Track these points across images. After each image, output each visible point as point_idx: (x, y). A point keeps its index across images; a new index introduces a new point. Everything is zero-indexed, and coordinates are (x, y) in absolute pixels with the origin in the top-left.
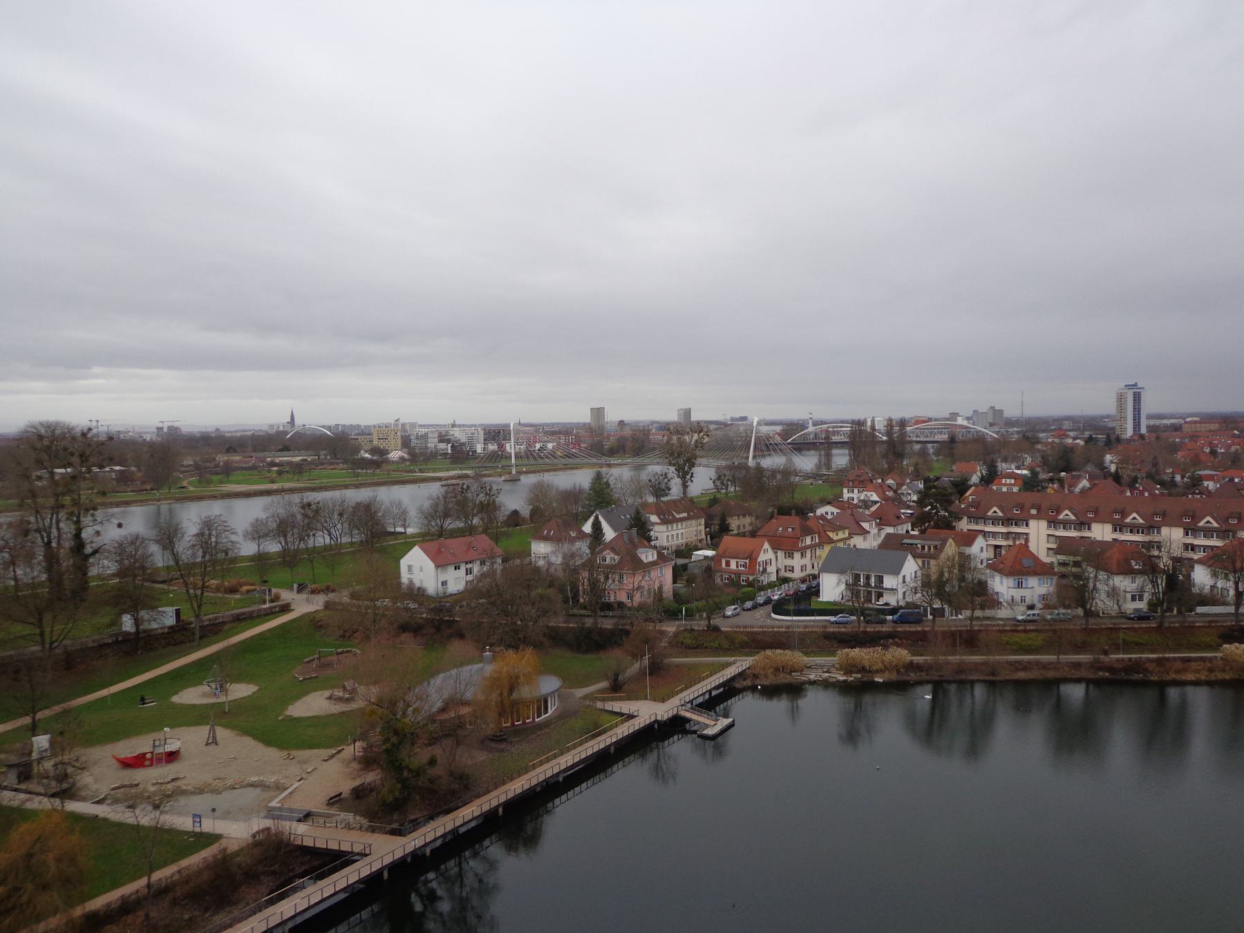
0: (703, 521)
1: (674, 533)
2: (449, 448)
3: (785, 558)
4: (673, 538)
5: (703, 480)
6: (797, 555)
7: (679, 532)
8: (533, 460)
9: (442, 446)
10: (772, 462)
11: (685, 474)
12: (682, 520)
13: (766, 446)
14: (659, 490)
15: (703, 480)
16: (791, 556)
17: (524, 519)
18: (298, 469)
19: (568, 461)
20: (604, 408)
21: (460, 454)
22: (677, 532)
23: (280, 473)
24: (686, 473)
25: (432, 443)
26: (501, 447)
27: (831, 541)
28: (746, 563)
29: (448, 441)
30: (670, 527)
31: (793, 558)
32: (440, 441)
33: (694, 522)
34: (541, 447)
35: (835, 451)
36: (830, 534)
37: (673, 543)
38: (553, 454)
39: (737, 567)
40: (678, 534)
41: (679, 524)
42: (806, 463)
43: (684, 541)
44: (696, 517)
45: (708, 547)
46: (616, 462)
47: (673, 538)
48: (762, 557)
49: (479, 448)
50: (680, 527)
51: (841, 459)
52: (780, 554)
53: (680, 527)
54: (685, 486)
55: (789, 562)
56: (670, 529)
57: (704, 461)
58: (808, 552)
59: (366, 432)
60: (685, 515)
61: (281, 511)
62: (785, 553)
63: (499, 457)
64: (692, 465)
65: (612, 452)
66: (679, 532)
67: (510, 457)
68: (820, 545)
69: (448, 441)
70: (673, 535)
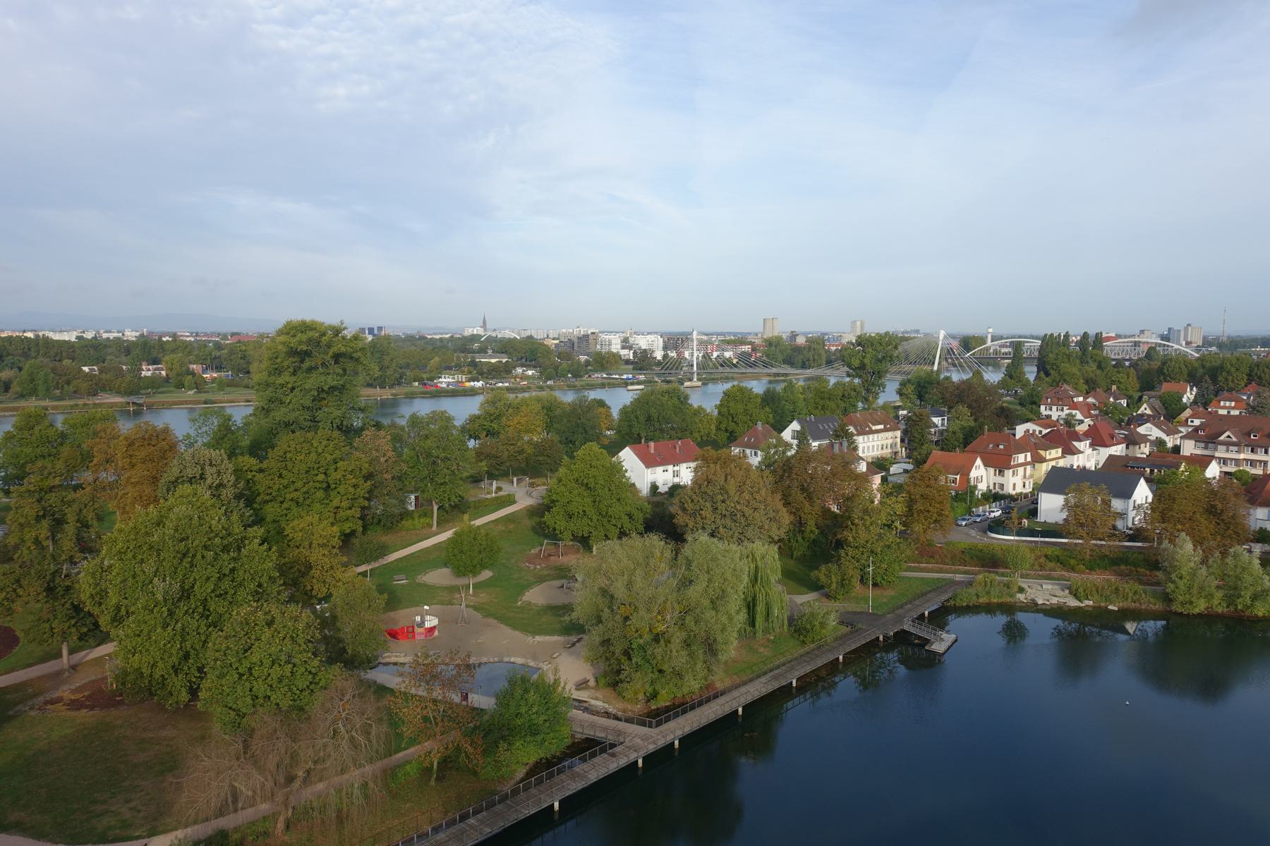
1: (870, 444)
2: (631, 355)
3: (995, 475)
4: (868, 449)
6: (1009, 473)
7: (875, 444)
8: (711, 370)
16: (1001, 473)
21: (643, 361)
22: (873, 443)
28: (956, 479)
30: (866, 437)
31: (1003, 476)
33: (890, 434)
34: (718, 356)
36: (1042, 452)
37: (869, 454)
39: (946, 482)
40: (873, 446)
41: (876, 435)
43: (879, 453)
46: (795, 372)
47: (868, 449)
48: (974, 474)
49: (659, 355)
50: (876, 439)
52: (992, 470)
53: (876, 439)
55: (999, 480)
56: (866, 441)
60: (881, 427)
62: (995, 470)
63: (678, 364)
66: (875, 444)
67: (692, 365)
70: (869, 447)
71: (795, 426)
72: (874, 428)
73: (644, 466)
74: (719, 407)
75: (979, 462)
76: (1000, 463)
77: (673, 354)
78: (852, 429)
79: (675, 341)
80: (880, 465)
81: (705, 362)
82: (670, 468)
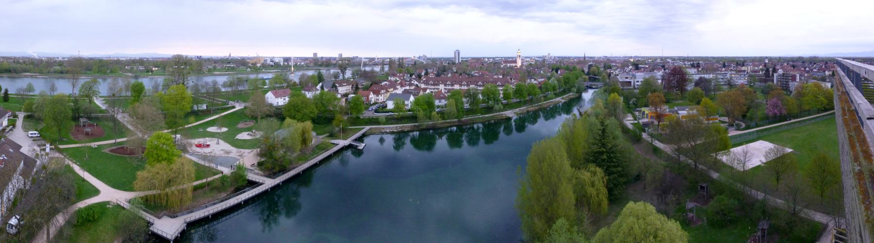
0: (351, 86)
5: (348, 74)
8: (298, 67)
9: (271, 63)
10: (368, 69)
11: (343, 73)
12: (345, 86)
13: (365, 65)
14: (336, 76)
15: (348, 74)
16: (378, 96)
17: (297, 85)
18: (233, 69)
19: (308, 67)
20: (314, 54)
21: (276, 65)
23: (228, 69)
24: (344, 72)
25: (268, 62)
26: (288, 63)
27: (388, 92)
29: (273, 62)
32: (271, 62)
33: (348, 86)
35: (385, 66)
38: (302, 66)
42: (377, 69)
44: (349, 85)
45: (354, 93)
48: (370, 96)
49: (282, 64)
51: (386, 68)
52: (375, 95)
54: (343, 75)
55: (377, 98)
57: (349, 68)
58: (383, 95)
59: (249, 58)
61: (232, 80)
64: (346, 70)
65: (320, 65)
68: (386, 93)
69: (273, 62)
71: (320, 84)
72: (344, 84)
73: (274, 97)
74: (299, 79)
75: (372, 93)
76: (377, 93)
77: (286, 64)
78: (337, 85)
79: (287, 60)
80: (346, 95)
81: (296, 66)
82: (283, 98)
